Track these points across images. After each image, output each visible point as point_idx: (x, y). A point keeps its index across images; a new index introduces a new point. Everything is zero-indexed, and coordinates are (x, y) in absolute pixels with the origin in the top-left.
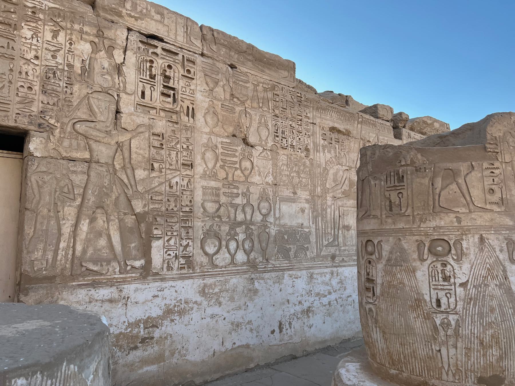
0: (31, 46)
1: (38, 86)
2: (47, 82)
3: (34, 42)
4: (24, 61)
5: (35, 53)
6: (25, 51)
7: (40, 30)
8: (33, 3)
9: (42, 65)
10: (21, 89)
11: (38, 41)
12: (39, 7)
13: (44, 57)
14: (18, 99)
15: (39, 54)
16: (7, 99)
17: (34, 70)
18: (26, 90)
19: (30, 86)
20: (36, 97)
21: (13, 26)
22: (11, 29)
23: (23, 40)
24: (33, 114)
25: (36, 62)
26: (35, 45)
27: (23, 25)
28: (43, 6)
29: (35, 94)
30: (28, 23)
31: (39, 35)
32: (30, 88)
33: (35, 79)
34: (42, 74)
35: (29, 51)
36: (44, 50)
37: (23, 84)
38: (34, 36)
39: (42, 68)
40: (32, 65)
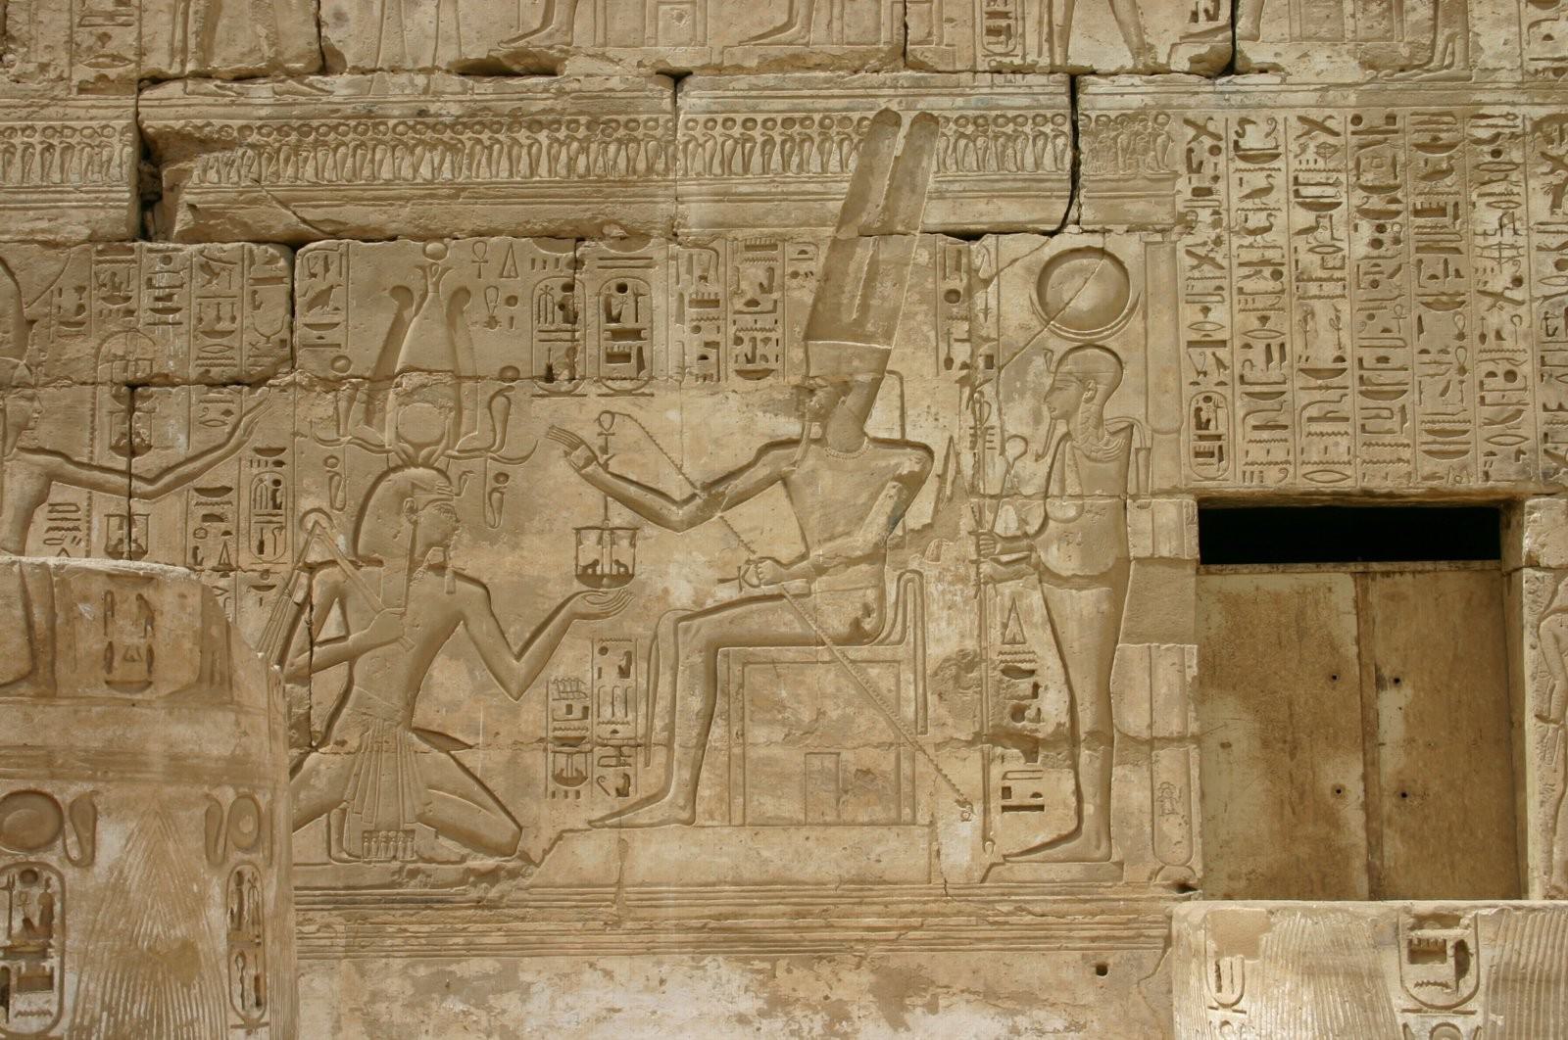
0: (1500, 249)
1: (1530, 362)
2: (1552, 346)
3: (1508, 237)
4: (1489, 301)
5: (1514, 269)
6: (1489, 270)
7: (1516, 199)
8: (1493, 126)
9: (1533, 300)
10: (1490, 383)
11: (1516, 232)
12: (1507, 131)
13: (1537, 272)
14: (1487, 412)
15: (1523, 271)
16: (1460, 417)
17: (1516, 319)
18: (1499, 382)
19: (1509, 367)
20: (1527, 397)
21: (1450, 210)
22: (1447, 220)
23: (1480, 241)
24: (1524, 446)
25: (1517, 294)
26: (1512, 247)
27: (1474, 197)
28: (1518, 122)
29: (1525, 389)
30: (1487, 189)
31: (1518, 212)
32: (1511, 375)
33: (1522, 345)
34: (1537, 324)
35: (1496, 268)
36: (1533, 252)
37: (1491, 367)
38: (1505, 221)
39: (1536, 304)
40: (1509, 309)
